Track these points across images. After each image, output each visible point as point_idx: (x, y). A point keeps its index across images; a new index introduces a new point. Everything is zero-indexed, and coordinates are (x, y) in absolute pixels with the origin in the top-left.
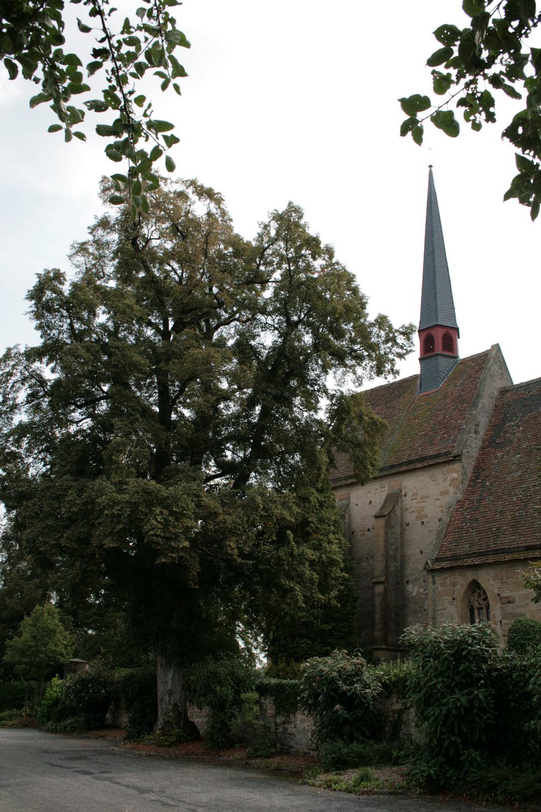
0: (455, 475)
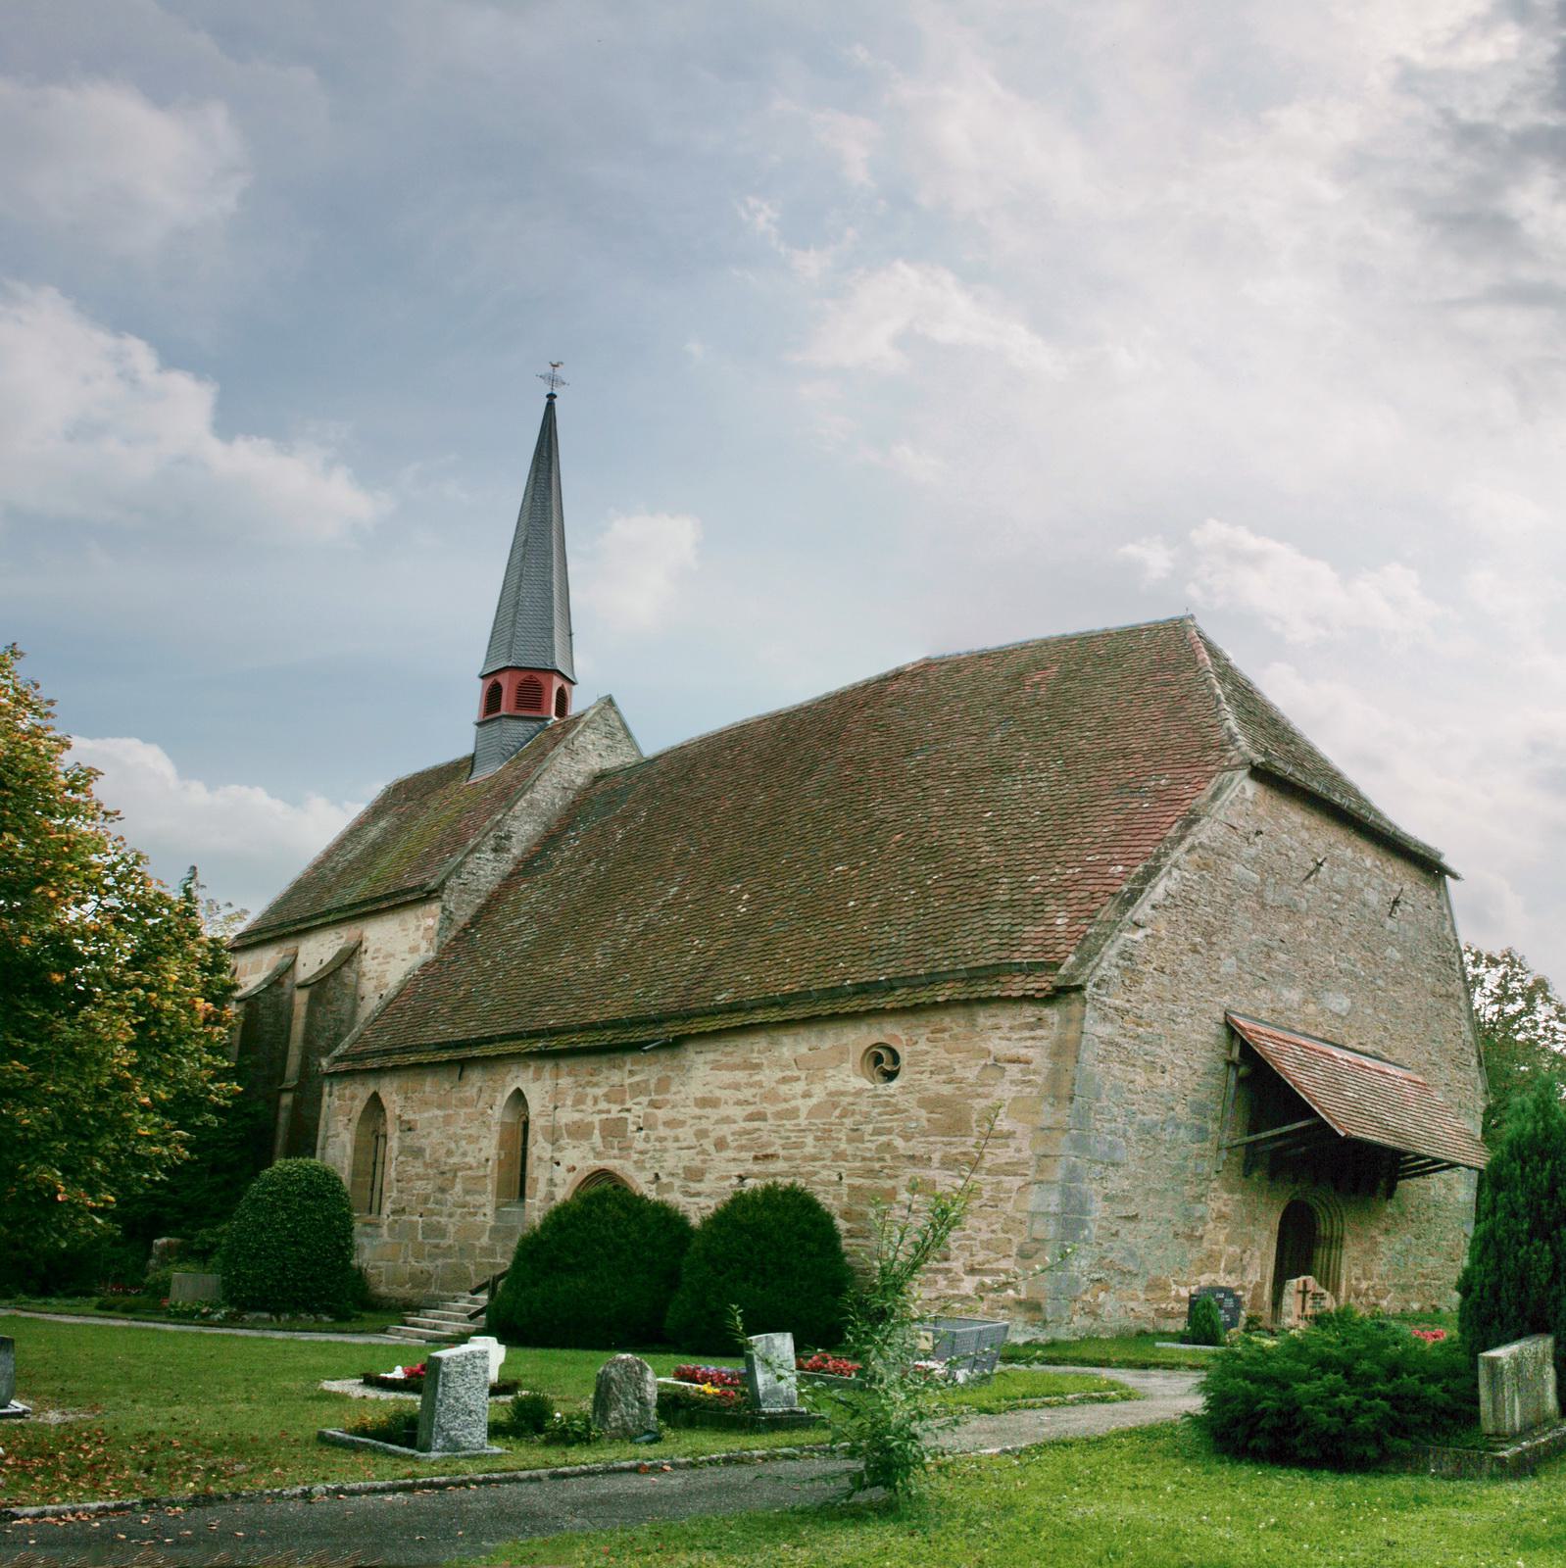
0: (430, 922)
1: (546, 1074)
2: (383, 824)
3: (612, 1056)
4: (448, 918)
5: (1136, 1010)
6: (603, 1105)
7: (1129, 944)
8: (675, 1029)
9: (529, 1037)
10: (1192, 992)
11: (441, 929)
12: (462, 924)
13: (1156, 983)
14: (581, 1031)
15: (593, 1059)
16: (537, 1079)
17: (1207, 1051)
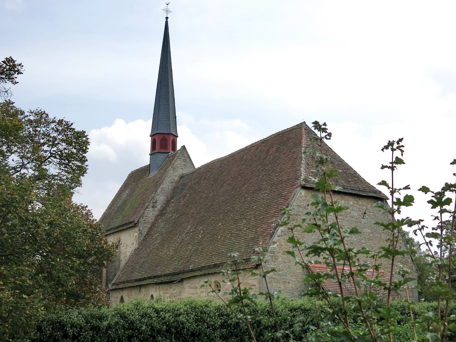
1: (158, 290)
2: (127, 192)
3: (170, 284)
4: (141, 233)
7: (272, 249)
8: (181, 276)
9: (154, 278)
11: (139, 237)
12: (144, 234)
14: (164, 276)
16: (156, 291)
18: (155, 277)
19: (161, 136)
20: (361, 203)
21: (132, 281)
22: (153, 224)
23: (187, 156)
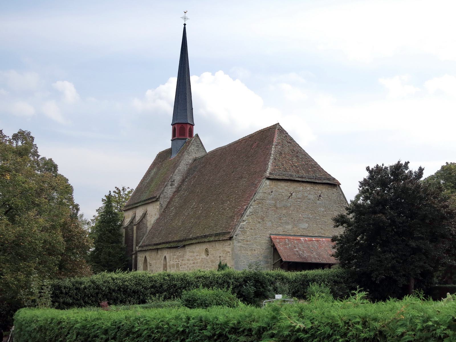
4: (161, 206)
5: (246, 239)
6: (176, 260)
7: (242, 225)
10: (260, 232)
11: (160, 209)
12: (164, 207)
13: (250, 232)
15: (175, 249)
16: (168, 254)
17: (266, 244)
18: (167, 243)
19: (180, 125)
20: (317, 188)
21: (152, 245)
22: (171, 199)
23: (199, 142)
